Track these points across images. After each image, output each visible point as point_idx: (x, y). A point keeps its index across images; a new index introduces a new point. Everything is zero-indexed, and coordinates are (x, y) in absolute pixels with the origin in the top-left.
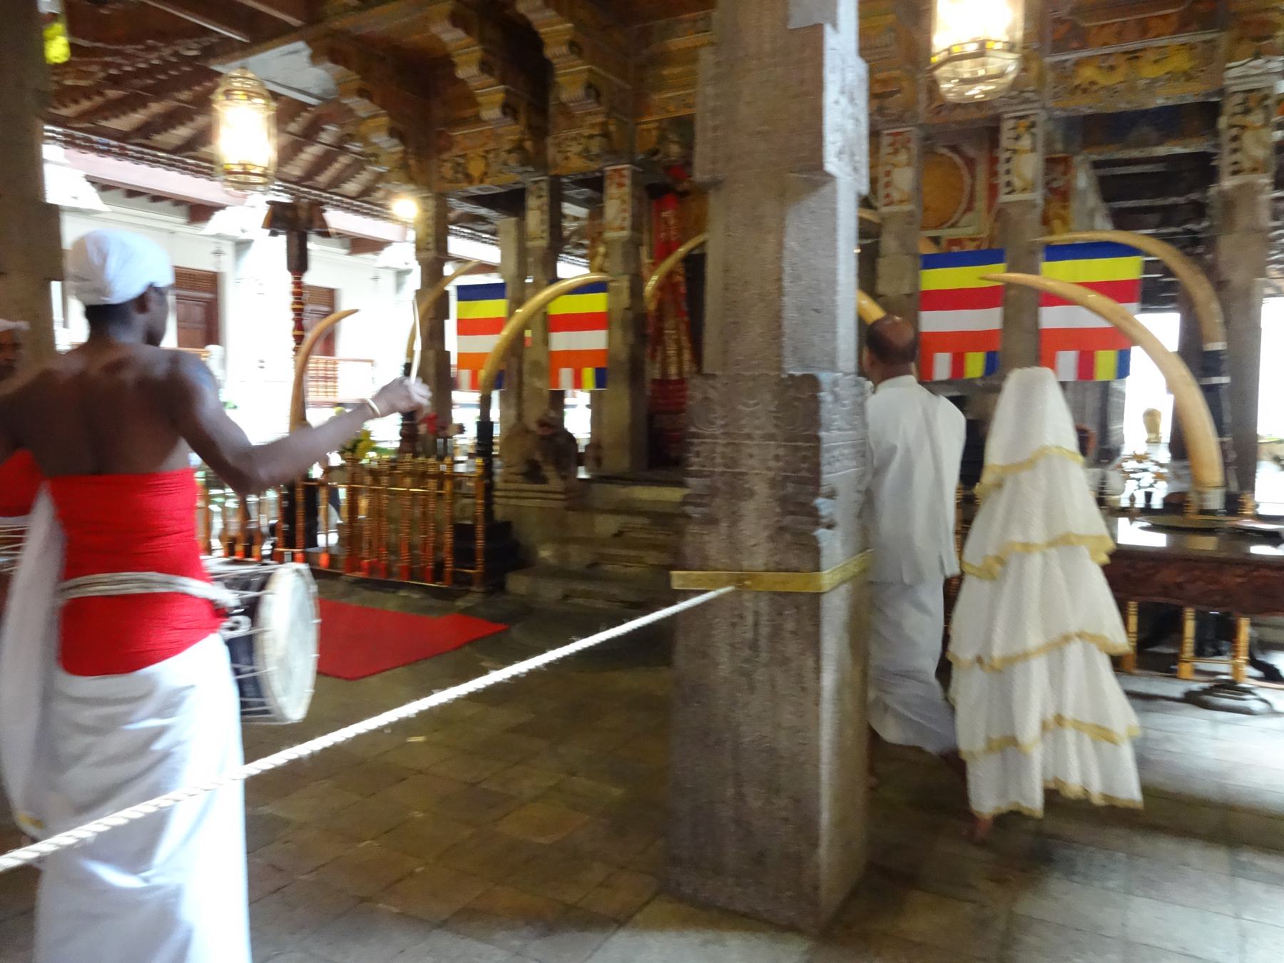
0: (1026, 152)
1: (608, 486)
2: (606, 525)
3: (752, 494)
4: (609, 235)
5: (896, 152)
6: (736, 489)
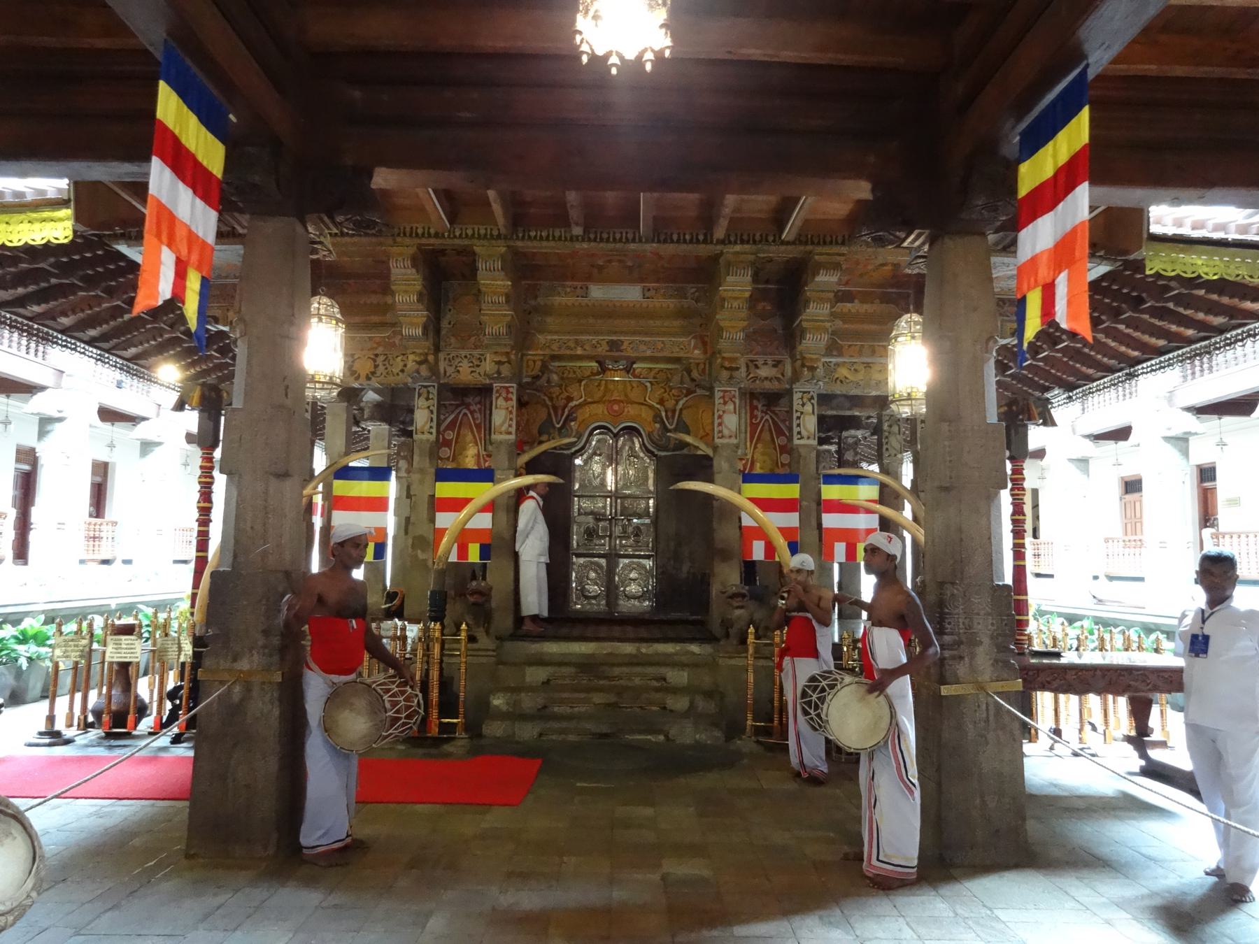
2: (536, 675)
5: (725, 403)
6: (974, 642)
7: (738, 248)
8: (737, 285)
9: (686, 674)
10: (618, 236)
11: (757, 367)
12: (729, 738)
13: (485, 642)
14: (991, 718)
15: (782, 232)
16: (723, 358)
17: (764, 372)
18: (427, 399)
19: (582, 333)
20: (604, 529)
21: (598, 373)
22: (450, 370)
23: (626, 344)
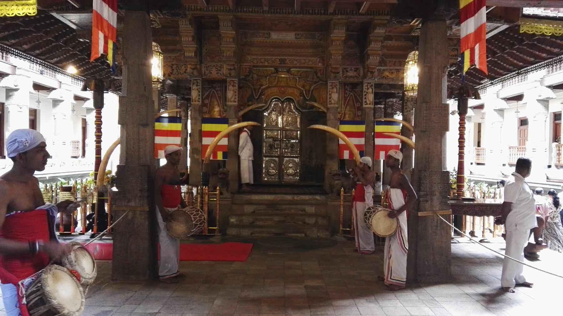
1: (243, 196)
2: (249, 209)
3: (436, 195)
4: (229, 103)
5: (332, 88)
6: (432, 194)
7: (339, 17)
8: (339, 34)
9: (314, 208)
10: (284, 11)
11: (347, 71)
12: (332, 236)
13: (226, 195)
14: (439, 225)
15: (359, 10)
16: (332, 68)
17: (351, 74)
18: (197, 86)
19: (268, 55)
20: (278, 145)
21: (274, 73)
22: (207, 72)
23: (288, 60)
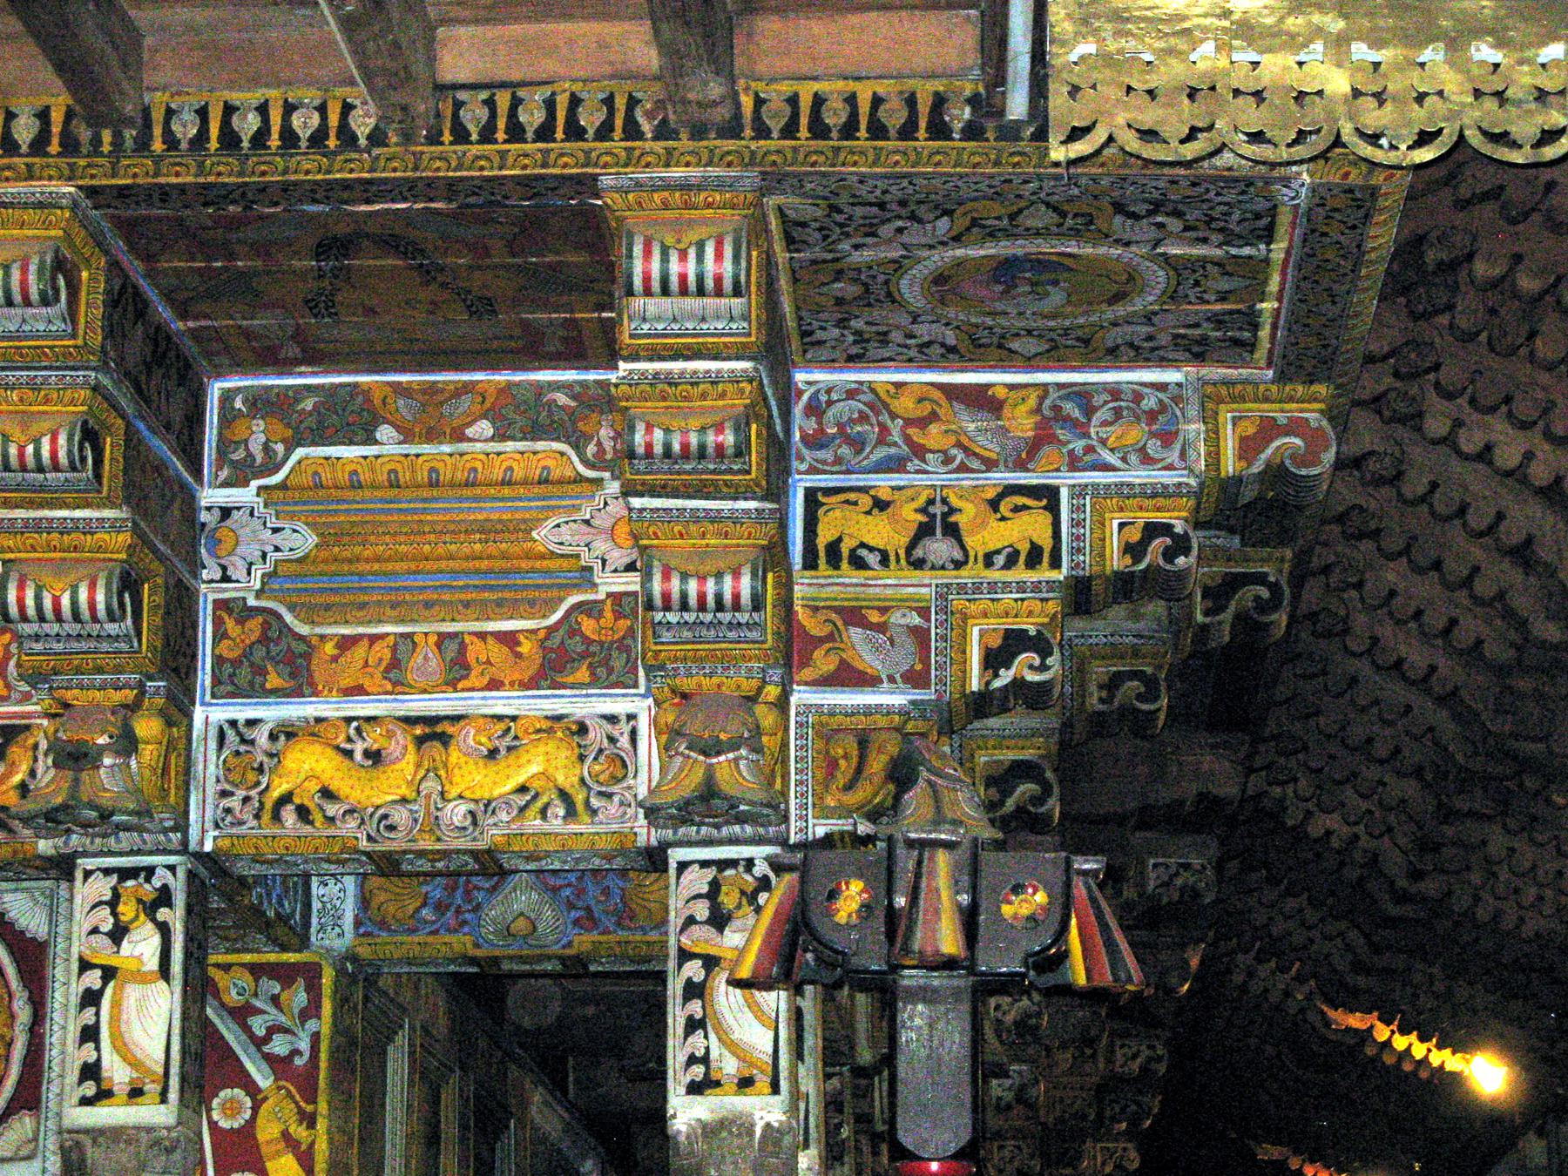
0: (141, 978)
